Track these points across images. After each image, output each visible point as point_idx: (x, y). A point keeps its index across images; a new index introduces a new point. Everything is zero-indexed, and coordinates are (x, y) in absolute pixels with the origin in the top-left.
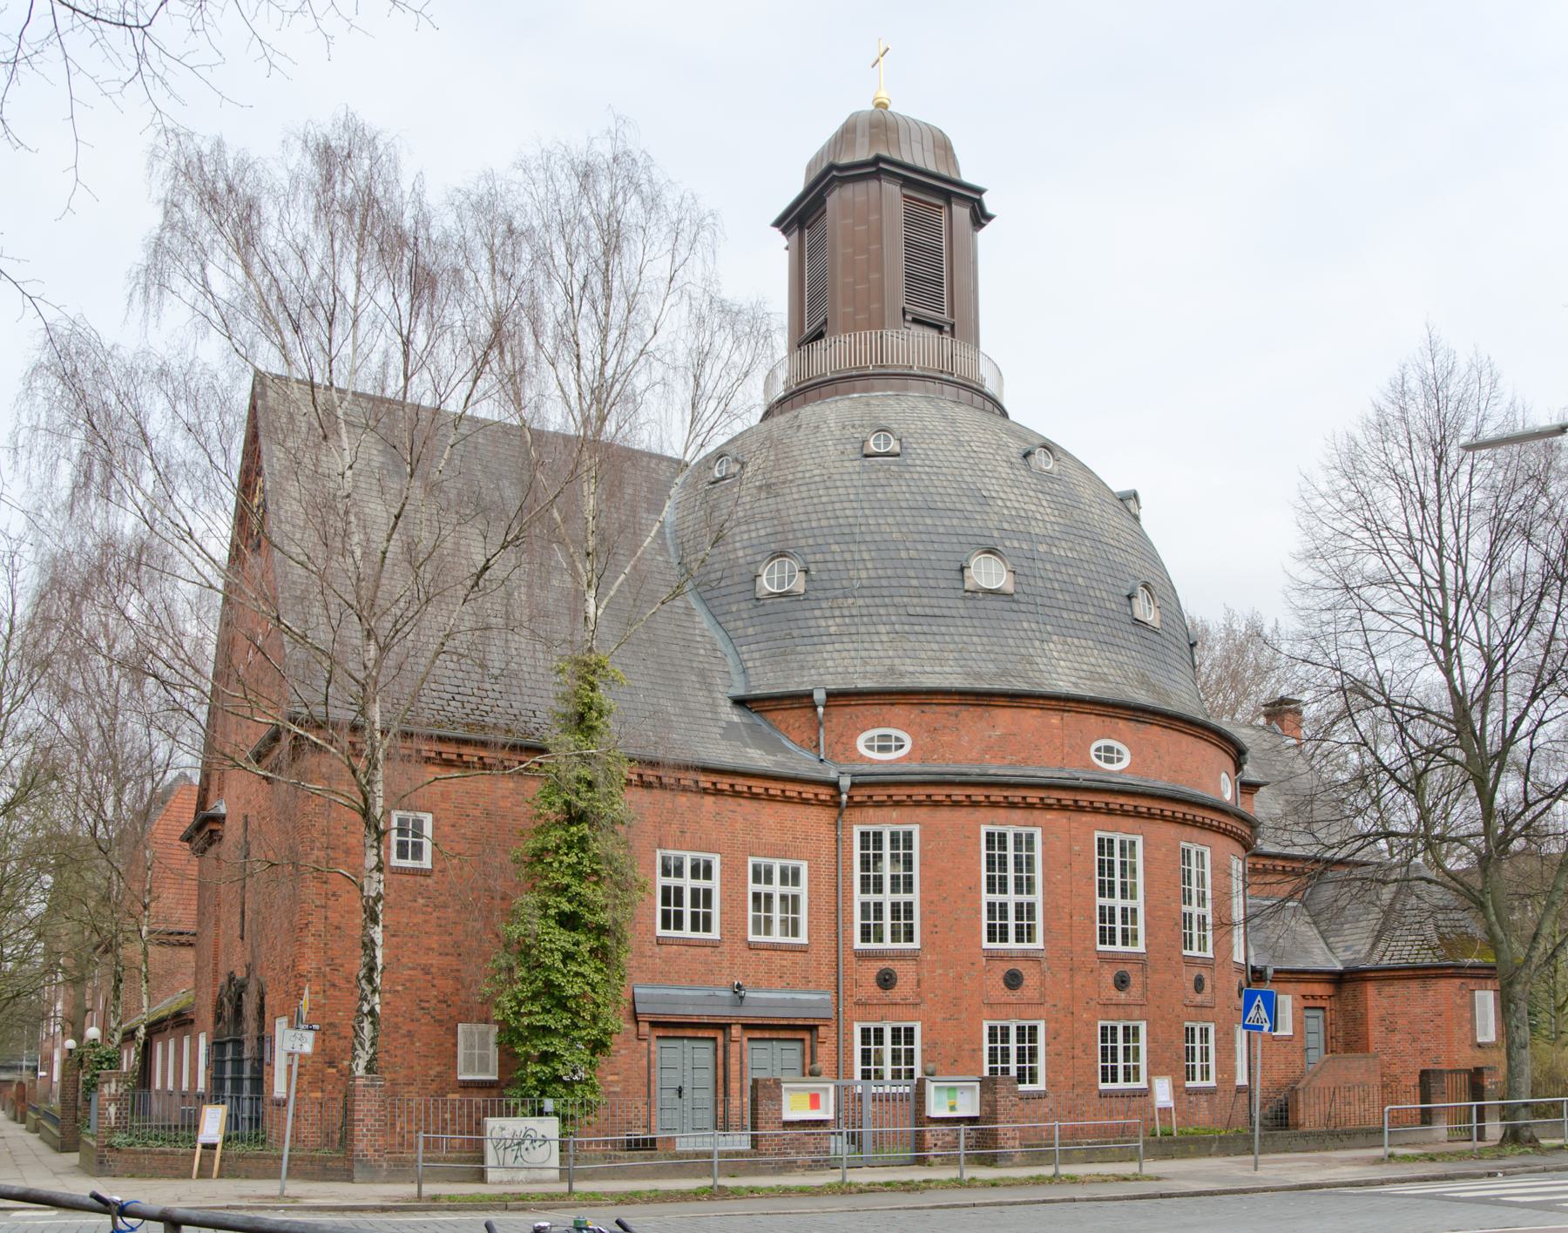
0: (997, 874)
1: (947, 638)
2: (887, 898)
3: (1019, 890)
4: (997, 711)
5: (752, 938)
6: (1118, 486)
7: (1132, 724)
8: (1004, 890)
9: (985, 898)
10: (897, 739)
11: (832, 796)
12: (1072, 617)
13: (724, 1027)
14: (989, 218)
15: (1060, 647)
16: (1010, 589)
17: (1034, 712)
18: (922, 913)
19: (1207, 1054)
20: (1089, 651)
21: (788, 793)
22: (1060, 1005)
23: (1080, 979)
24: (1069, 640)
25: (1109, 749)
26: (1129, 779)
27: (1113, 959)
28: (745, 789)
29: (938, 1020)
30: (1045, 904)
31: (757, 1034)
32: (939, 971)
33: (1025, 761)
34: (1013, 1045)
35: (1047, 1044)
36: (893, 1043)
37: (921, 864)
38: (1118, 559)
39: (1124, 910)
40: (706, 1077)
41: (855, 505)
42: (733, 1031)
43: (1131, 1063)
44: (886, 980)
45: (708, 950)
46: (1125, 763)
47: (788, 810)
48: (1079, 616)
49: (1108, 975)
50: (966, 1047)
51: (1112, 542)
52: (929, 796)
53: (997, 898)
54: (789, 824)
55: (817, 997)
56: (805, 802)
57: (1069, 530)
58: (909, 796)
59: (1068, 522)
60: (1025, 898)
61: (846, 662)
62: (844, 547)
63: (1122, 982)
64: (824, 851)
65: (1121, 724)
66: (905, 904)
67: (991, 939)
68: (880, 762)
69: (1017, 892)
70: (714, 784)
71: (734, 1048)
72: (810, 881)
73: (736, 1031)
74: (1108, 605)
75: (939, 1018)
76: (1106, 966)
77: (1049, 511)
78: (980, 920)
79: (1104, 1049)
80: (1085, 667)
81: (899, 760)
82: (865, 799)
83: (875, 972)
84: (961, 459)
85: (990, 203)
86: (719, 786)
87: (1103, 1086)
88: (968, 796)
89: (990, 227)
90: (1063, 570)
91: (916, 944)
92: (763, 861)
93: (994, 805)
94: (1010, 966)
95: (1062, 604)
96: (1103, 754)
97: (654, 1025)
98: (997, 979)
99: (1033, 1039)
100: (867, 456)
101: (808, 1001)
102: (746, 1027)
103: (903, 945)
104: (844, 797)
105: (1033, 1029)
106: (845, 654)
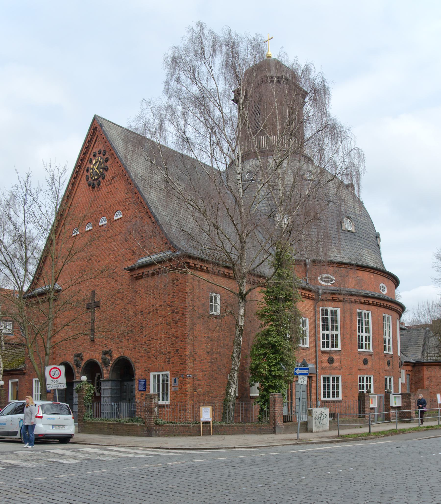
7: (387, 279)
17: (367, 273)
22: (377, 371)
30: (373, 337)
32: (346, 358)
35: (374, 384)
36: (333, 383)
44: (331, 361)
53: (360, 334)
83: (327, 358)
94: (364, 357)
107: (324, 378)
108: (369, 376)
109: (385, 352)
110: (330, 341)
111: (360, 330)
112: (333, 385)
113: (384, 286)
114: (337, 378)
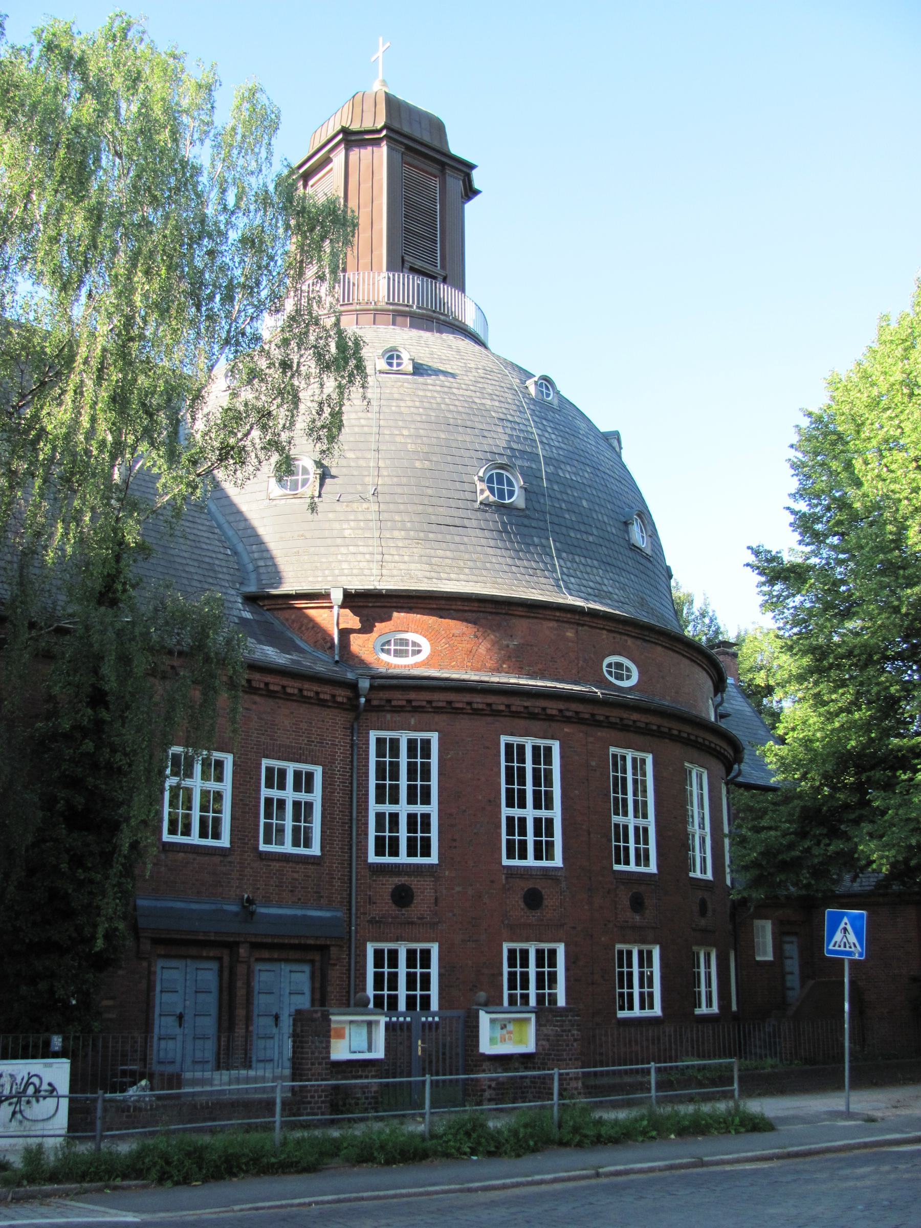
2: (403, 809)
3: (537, 806)
4: (515, 621)
5: (263, 847)
6: (603, 427)
7: (639, 642)
8: (523, 805)
9: (506, 812)
10: (414, 644)
11: (349, 699)
12: (579, 536)
13: (232, 946)
14: (476, 192)
15: (569, 564)
16: (521, 504)
20: (595, 571)
21: (305, 693)
24: (577, 559)
25: (619, 666)
28: (262, 686)
31: (266, 954)
32: (458, 889)
34: (532, 970)
35: (567, 969)
37: (440, 774)
38: (614, 488)
40: (210, 1001)
42: (241, 951)
43: (646, 990)
44: (402, 896)
45: (217, 859)
46: (634, 680)
47: (302, 710)
48: (585, 537)
51: (608, 471)
52: (450, 703)
53: (516, 812)
54: (304, 726)
55: (328, 914)
56: (322, 703)
57: (571, 455)
58: (430, 702)
59: (570, 448)
60: (543, 813)
61: (362, 565)
62: (359, 454)
63: (637, 904)
64: (339, 757)
65: (630, 641)
66: (422, 815)
67: (510, 856)
68: (397, 666)
71: (241, 969)
72: (324, 788)
73: (243, 951)
74: (609, 529)
76: (623, 887)
77: (553, 436)
80: (591, 584)
81: (416, 665)
82: (383, 703)
83: (390, 888)
84: (470, 383)
88: (489, 705)
89: (476, 200)
90: (569, 492)
92: (277, 764)
93: (515, 715)
94: (530, 885)
95: (569, 524)
97: (156, 941)
98: (516, 901)
99: (553, 964)
101: (320, 918)
102: (255, 946)
103: (419, 860)
104: (363, 700)
106: (360, 557)
107: (378, 954)
108: (546, 946)
109: (617, 867)
110: (403, 834)
111: (516, 799)
112: (408, 974)
113: (626, 662)
114: (426, 954)
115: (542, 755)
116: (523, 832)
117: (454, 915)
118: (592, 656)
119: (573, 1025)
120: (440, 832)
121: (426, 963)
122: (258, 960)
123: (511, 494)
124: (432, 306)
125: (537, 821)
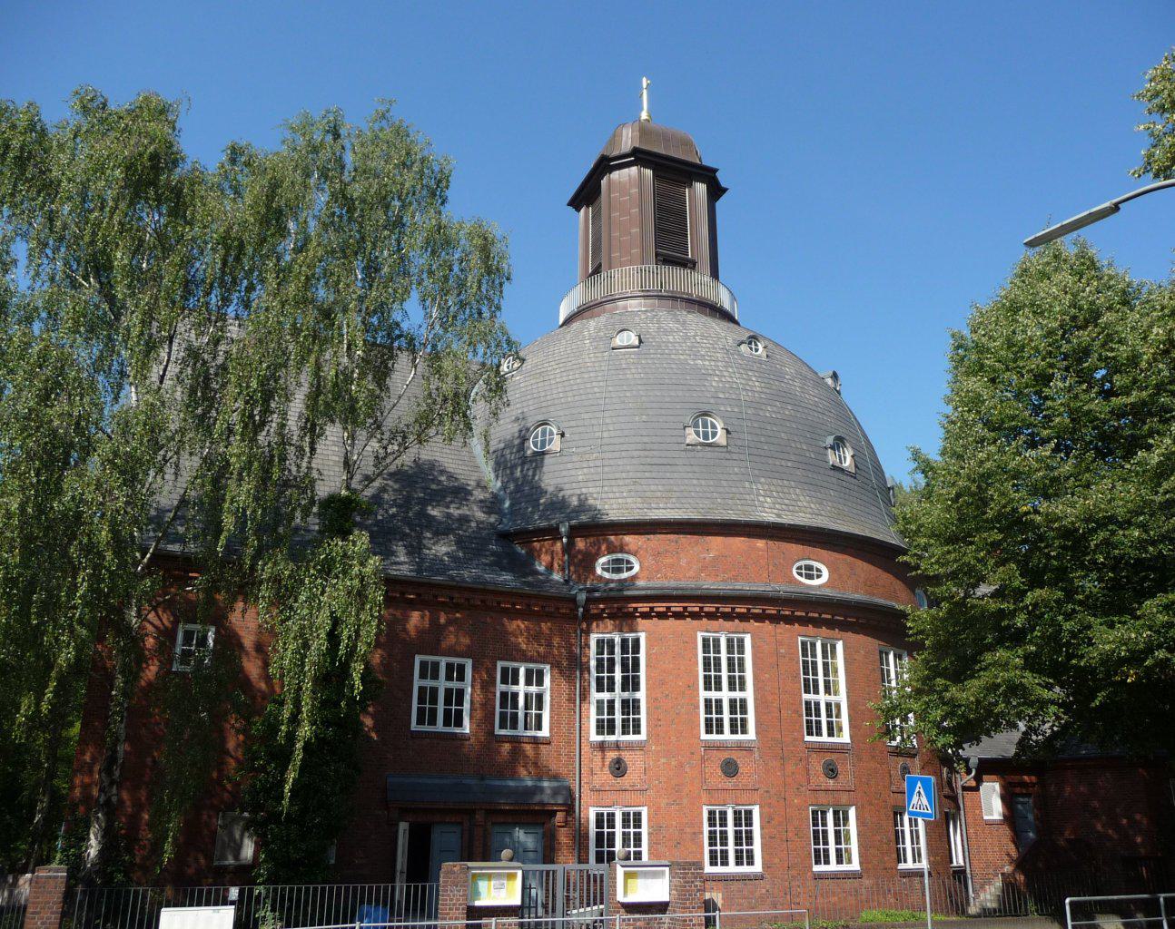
0: (713, 673)
1: (672, 482)
8: (719, 688)
11: (571, 610)
13: (471, 812)
14: (725, 190)
18: (648, 708)
19: (918, 838)
22: (773, 791)
23: (791, 768)
26: (829, 592)
27: (822, 749)
29: (662, 805)
30: (756, 699)
32: (663, 760)
33: (735, 578)
34: (730, 829)
35: (762, 828)
36: (624, 827)
37: (647, 666)
39: (828, 705)
41: (601, 384)
44: (619, 768)
49: (817, 765)
50: (688, 830)
53: (713, 695)
60: (737, 695)
67: (709, 731)
69: (730, 690)
70: (468, 600)
75: (663, 803)
77: (757, 384)
78: (698, 715)
79: (816, 832)
85: (724, 181)
86: (472, 602)
87: (816, 868)
91: (643, 736)
94: (726, 755)
96: (803, 571)
100: (613, 349)
104: (581, 610)
105: (749, 813)
111: (712, 683)
114: (638, 816)
115: (736, 646)
116: (719, 711)
117: (660, 782)
118: (781, 561)
119: (696, 878)
120: (648, 714)
121: (638, 824)
122: (493, 824)
123: (714, 434)
124: (677, 288)
125: (733, 702)
